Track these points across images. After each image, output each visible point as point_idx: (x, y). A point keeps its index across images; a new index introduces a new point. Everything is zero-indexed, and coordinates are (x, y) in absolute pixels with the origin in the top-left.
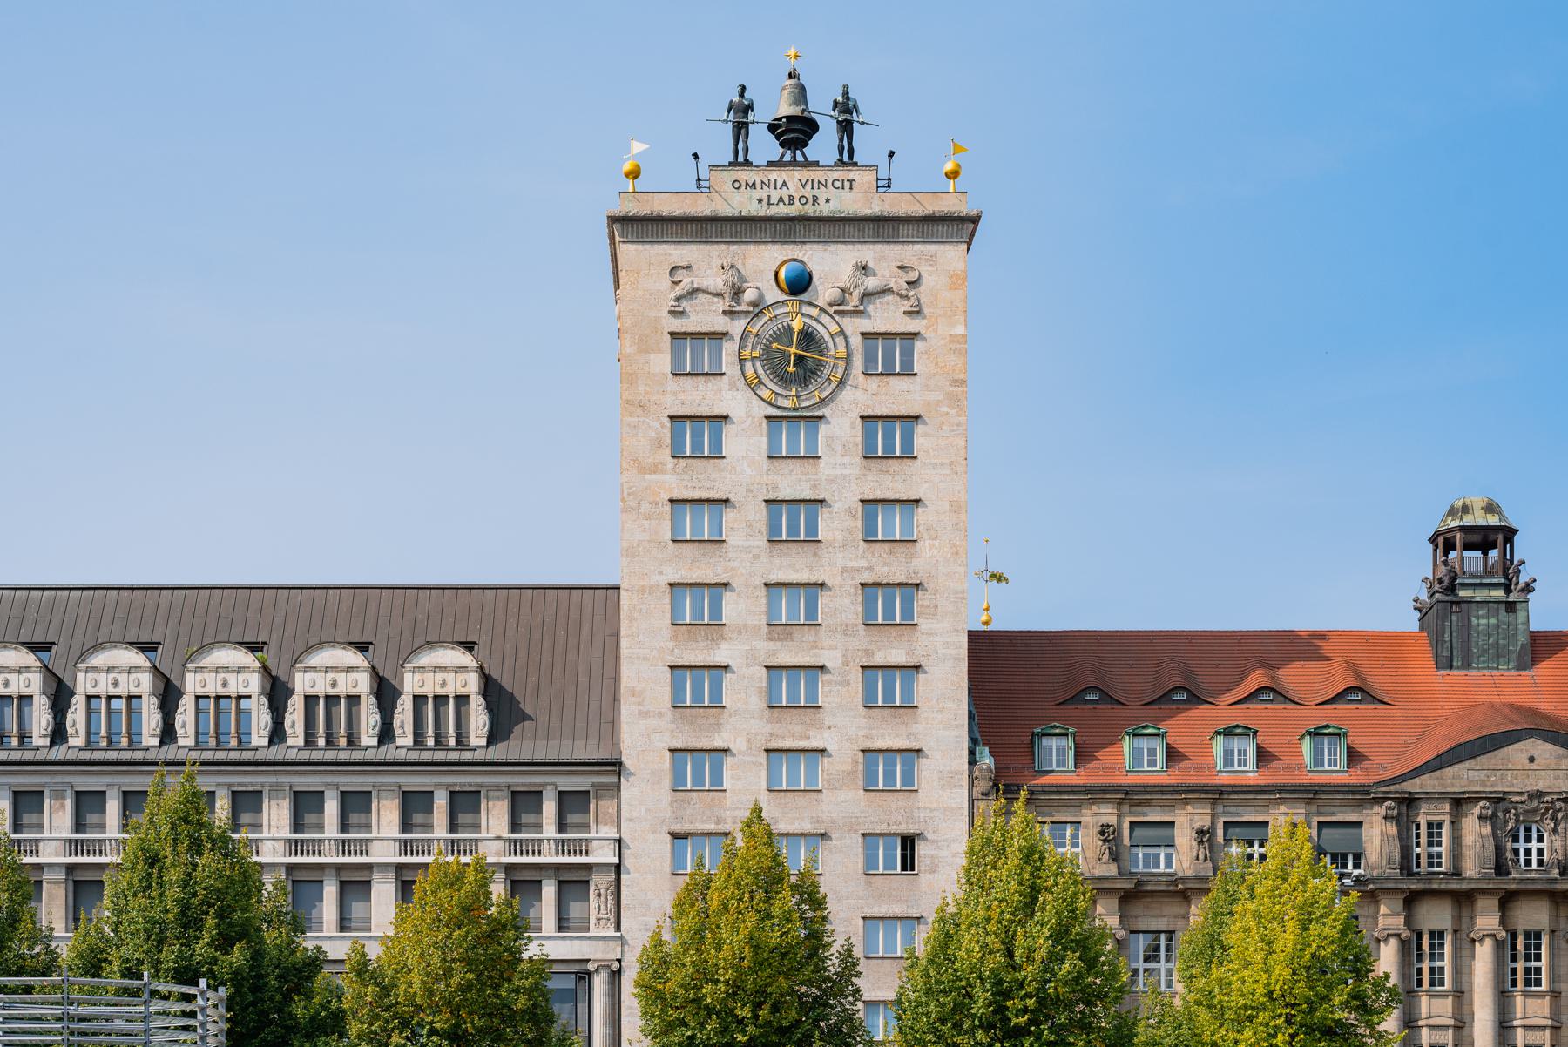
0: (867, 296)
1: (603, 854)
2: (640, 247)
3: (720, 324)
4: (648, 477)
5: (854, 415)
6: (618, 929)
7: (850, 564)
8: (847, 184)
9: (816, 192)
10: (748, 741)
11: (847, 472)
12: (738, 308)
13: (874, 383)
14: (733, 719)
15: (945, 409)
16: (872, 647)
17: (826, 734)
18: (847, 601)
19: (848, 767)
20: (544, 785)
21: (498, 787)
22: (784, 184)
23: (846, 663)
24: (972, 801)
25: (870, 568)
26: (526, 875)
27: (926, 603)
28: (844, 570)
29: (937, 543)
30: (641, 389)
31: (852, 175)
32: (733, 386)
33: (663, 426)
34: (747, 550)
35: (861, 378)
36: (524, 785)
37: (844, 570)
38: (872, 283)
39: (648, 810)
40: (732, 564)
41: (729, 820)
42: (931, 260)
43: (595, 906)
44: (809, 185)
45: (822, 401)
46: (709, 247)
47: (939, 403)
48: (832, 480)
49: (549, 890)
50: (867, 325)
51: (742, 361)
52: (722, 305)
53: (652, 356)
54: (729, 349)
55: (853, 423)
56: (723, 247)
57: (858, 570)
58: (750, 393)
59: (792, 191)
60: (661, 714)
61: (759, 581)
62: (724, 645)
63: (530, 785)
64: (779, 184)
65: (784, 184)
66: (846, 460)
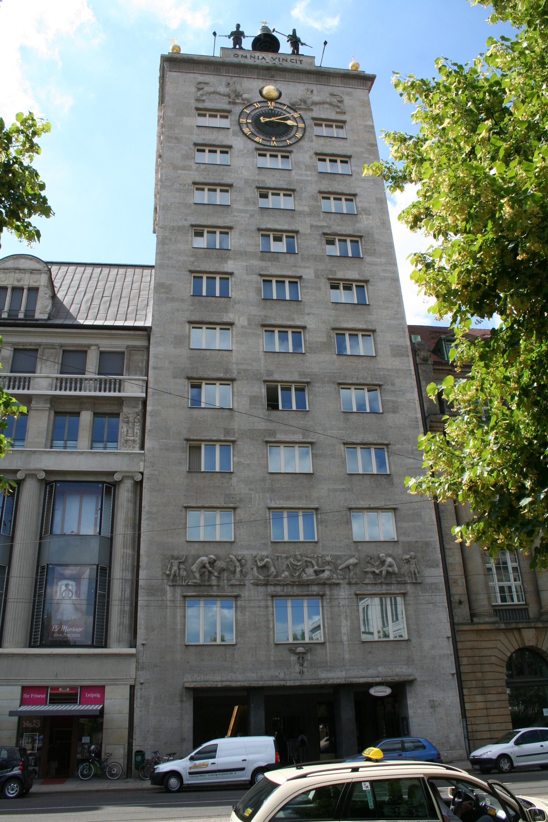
0: (315, 103)
1: (132, 390)
2: (179, 74)
3: (227, 107)
4: (179, 172)
5: (312, 153)
6: (142, 447)
7: (314, 223)
8: (298, 62)
9: (281, 62)
10: (249, 320)
11: (309, 178)
12: (237, 101)
13: (322, 141)
14: (236, 306)
15: (367, 156)
16: (334, 269)
17: (306, 318)
18: (315, 243)
19: (324, 340)
20: (89, 346)
21: (52, 346)
22: (263, 58)
23: (317, 277)
24: (416, 365)
25: (329, 227)
26: (69, 408)
27: (369, 247)
28: (312, 226)
29: (371, 217)
30: (177, 131)
31: (301, 59)
32: (235, 134)
33: (190, 149)
34: (245, 211)
35: (314, 138)
36: (73, 345)
37: (312, 226)
38: (316, 98)
39: (170, 362)
40: (235, 218)
41: (235, 372)
42: (349, 94)
43: (127, 430)
44: (277, 60)
45: (291, 145)
46: (220, 77)
47: (362, 152)
48: (299, 182)
49: (86, 417)
50: (315, 114)
51: (240, 124)
52: (226, 100)
53: (185, 118)
54: (234, 117)
55: (311, 157)
56: (229, 78)
57: (322, 227)
58: (245, 138)
59: (268, 60)
60: (183, 300)
61: (254, 228)
62: (230, 262)
63: (79, 345)
64: (260, 57)
65: (263, 58)
66: (308, 173)
